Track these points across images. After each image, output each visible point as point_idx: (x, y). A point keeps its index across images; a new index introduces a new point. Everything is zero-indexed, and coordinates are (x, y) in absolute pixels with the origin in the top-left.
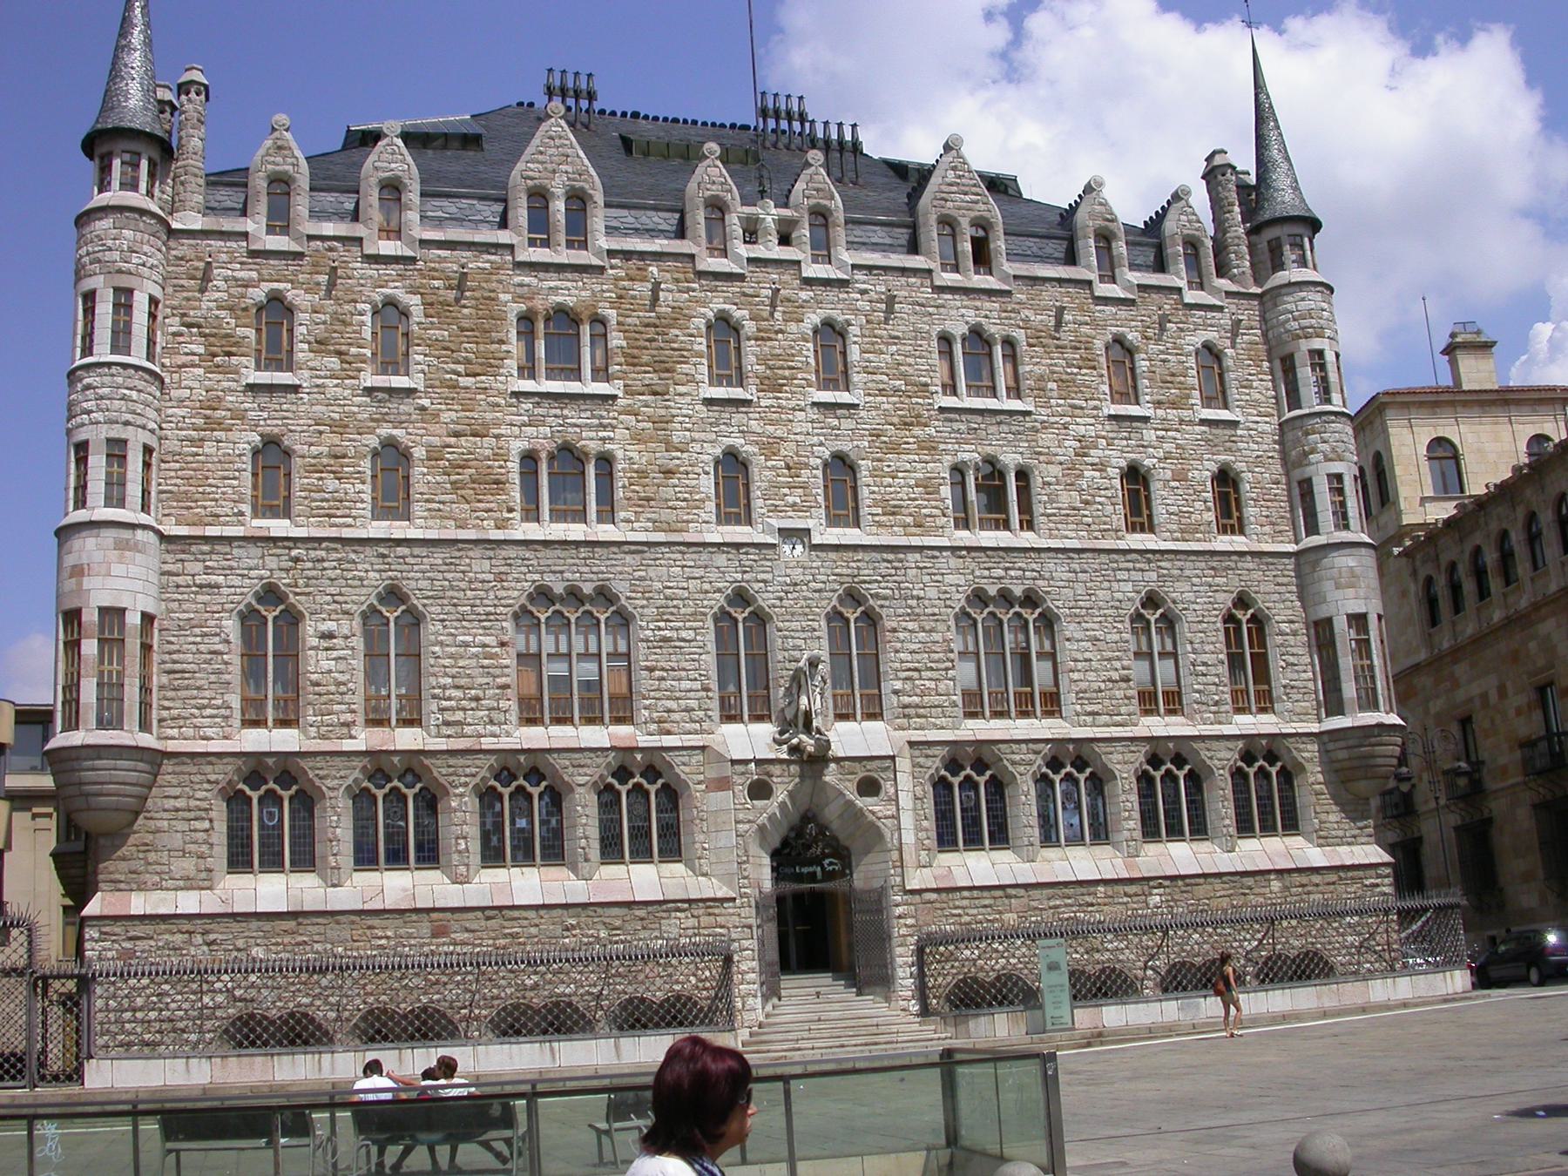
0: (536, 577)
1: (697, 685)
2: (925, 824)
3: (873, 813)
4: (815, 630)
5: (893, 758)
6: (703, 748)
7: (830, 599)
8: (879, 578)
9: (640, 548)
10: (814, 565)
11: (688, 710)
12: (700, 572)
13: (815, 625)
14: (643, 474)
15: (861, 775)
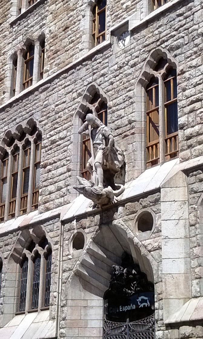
0: (6, 128)
1: (64, 169)
2: (196, 250)
3: (146, 247)
4: (130, 98)
5: (158, 190)
6: (58, 216)
7: (141, 68)
8: (174, 33)
9: (46, 86)
10: (132, 46)
11: (59, 189)
12: (72, 87)
13: (130, 94)
14: (55, 37)
15: (139, 212)
